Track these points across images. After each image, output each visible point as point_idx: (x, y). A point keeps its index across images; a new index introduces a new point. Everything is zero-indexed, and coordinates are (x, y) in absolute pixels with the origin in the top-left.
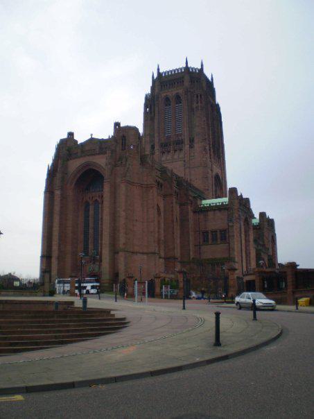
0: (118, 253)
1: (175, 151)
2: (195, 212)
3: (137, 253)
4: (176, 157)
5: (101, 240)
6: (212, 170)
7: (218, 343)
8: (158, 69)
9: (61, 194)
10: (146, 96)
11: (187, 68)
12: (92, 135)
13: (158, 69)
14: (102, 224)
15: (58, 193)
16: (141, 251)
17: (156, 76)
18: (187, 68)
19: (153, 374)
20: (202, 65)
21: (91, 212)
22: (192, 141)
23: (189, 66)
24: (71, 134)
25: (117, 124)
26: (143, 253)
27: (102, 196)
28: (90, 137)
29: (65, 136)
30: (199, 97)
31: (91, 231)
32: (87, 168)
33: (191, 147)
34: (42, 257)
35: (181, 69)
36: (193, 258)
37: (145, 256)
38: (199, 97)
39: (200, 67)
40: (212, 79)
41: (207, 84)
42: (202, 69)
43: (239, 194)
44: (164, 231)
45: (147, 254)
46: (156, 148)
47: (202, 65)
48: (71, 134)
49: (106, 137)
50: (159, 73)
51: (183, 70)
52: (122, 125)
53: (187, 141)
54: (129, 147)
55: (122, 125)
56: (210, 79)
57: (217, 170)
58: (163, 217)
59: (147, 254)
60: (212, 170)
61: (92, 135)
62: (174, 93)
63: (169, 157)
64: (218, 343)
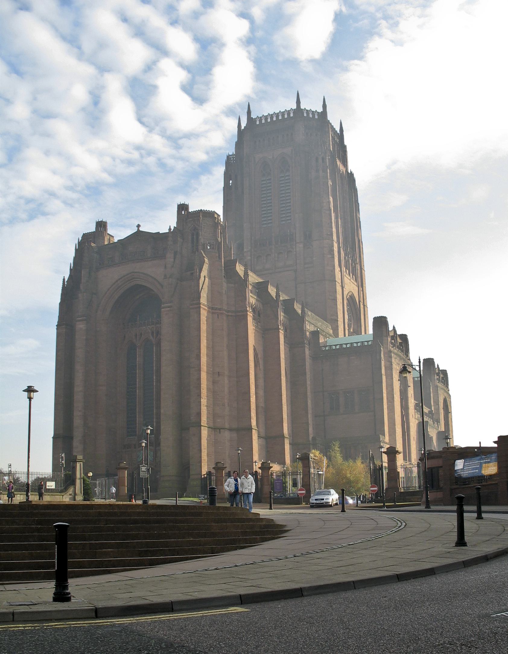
0: (188, 429)
2: (315, 358)
3: (220, 429)
5: (159, 407)
6: (343, 288)
7: (461, 542)
8: (249, 112)
11: (298, 110)
12: (139, 226)
13: (249, 112)
14: (159, 381)
15: (81, 326)
16: (227, 426)
17: (243, 125)
18: (298, 110)
19: (400, 578)
20: (324, 106)
21: (139, 360)
23: (302, 107)
24: (101, 225)
25: (182, 208)
26: (230, 430)
27: (158, 333)
28: (135, 230)
30: (320, 161)
31: (139, 392)
34: (56, 438)
35: (289, 112)
36: (314, 439)
37: (235, 435)
38: (320, 161)
39: (320, 110)
41: (333, 138)
42: (324, 114)
43: (391, 328)
44: (265, 392)
45: (238, 430)
46: (245, 250)
47: (324, 106)
48: (101, 225)
49: (164, 230)
50: (250, 119)
51: (292, 115)
52: (190, 211)
54: (204, 245)
56: (338, 132)
57: (351, 286)
58: (261, 367)
59: (238, 430)
60: (343, 288)
61: (139, 226)
64: (461, 542)
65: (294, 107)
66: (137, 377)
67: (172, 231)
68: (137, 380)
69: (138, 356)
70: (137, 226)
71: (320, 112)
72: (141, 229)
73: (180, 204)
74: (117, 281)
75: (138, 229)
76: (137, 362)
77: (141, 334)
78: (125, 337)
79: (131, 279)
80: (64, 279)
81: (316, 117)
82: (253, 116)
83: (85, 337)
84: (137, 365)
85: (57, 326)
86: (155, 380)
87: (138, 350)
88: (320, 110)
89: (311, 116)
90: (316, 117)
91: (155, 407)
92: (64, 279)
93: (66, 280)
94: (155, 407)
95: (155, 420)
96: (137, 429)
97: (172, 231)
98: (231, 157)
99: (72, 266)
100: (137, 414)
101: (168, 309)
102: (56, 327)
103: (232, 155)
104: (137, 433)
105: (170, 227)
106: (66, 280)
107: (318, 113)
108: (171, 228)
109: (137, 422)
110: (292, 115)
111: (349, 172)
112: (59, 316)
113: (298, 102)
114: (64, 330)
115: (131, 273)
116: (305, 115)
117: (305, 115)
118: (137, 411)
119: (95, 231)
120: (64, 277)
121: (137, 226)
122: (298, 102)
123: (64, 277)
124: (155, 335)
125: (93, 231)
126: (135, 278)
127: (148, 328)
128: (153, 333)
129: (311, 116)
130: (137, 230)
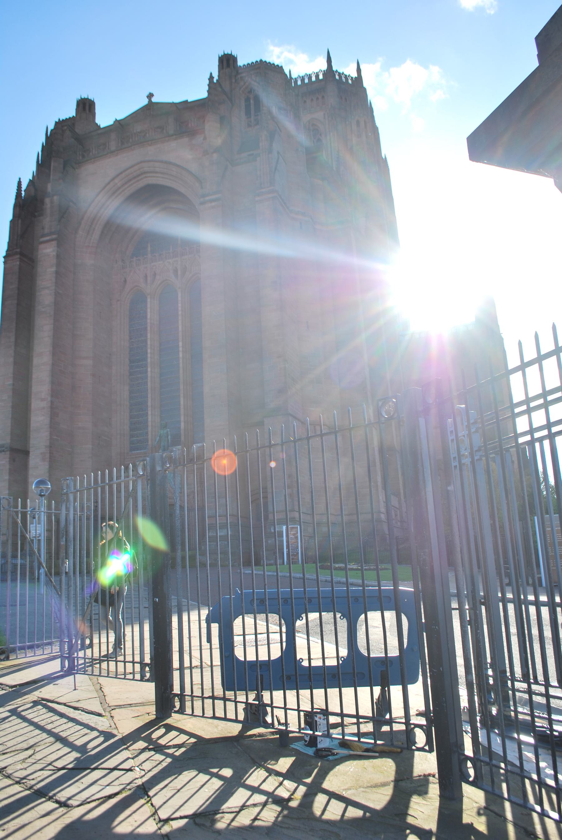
9: (58, 256)
11: (330, 72)
12: (150, 96)
18: (330, 72)
20: (359, 70)
28: (145, 102)
29: (70, 111)
32: (141, 184)
39: (354, 75)
42: (359, 80)
47: (359, 70)
51: (321, 77)
55: (241, 62)
61: (150, 96)
65: (324, 67)
66: (149, 346)
67: (215, 81)
68: (149, 351)
69: (149, 310)
70: (148, 97)
71: (354, 77)
72: (154, 100)
73: (223, 54)
74: (113, 179)
75: (150, 100)
76: (148, 321)
77: (155, 275)
78: (125, 281)
79: (138, 176)
80: (20, 183)
81: (350, 82)
83: (54, 269)
84: (149, 325)
85: (4, 257)
86: (181, 349)
87: (149, 300)
88: (354, 74)
89: (344, 79)
90: (350, 82)
91: (182, 395)
92: (20, 183)
93: (24, 187)
94: (182, 395)
95: (182, 418)
96: (150, 436)
97: (215, 81)
99: (35, 174)
100: (149, 409)
101: (213, 204)
102: (3, 260)
104: (150, 443)
105: (211, 74)
106: (24, 187)
107: (351, 77)
108: (213, 75)
109: (150, 424)
110: (321, 77)
111: (384, 157)
112: (8, 243)
114: (18, 263)
115: (138, 163)
116: (337, 77)
117: (337, 77)
118: (149, 404)
119: (75, 116)
120: (20, 179)
121: (148, 97)
123: (20, 179)
124: (179, 272)
125: (71, 116)
126: (147, 172)
127: (167, 262)
128: (176, 271)
129: (344, 79)
130: (149, 102)
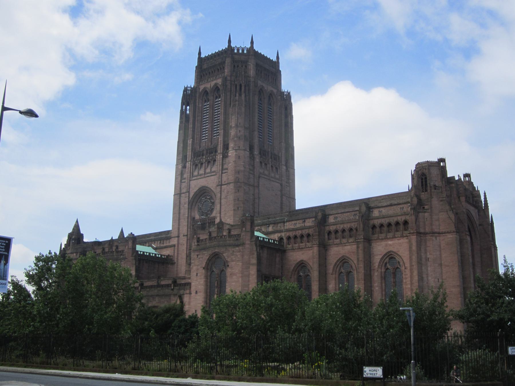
1: (209, 162)
4: (208, 170)
8: (200, 53)
10: (186, 90)
11: (230, 49)
13: (200, 53)
20: (252, 43)
22: (226, 147)
23: (233, 45)
33: (225, 156)
39: (249, 46)
40: (278, 58)
47: (252, 43)
53: (220, 149)
62: (213, 83)
63: (202, 172)
71: (249, 47)
81: (245, 52)
82: (203, 56)
89: (240, 51)
90: (245, 52)
98: (189, 88)
103: (190, 87)
113: (230, 41)
116: (236, 51)
117: (236, 51)
122: (230, 41)
129: (240, 51)
